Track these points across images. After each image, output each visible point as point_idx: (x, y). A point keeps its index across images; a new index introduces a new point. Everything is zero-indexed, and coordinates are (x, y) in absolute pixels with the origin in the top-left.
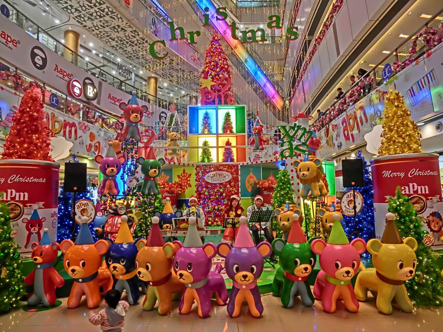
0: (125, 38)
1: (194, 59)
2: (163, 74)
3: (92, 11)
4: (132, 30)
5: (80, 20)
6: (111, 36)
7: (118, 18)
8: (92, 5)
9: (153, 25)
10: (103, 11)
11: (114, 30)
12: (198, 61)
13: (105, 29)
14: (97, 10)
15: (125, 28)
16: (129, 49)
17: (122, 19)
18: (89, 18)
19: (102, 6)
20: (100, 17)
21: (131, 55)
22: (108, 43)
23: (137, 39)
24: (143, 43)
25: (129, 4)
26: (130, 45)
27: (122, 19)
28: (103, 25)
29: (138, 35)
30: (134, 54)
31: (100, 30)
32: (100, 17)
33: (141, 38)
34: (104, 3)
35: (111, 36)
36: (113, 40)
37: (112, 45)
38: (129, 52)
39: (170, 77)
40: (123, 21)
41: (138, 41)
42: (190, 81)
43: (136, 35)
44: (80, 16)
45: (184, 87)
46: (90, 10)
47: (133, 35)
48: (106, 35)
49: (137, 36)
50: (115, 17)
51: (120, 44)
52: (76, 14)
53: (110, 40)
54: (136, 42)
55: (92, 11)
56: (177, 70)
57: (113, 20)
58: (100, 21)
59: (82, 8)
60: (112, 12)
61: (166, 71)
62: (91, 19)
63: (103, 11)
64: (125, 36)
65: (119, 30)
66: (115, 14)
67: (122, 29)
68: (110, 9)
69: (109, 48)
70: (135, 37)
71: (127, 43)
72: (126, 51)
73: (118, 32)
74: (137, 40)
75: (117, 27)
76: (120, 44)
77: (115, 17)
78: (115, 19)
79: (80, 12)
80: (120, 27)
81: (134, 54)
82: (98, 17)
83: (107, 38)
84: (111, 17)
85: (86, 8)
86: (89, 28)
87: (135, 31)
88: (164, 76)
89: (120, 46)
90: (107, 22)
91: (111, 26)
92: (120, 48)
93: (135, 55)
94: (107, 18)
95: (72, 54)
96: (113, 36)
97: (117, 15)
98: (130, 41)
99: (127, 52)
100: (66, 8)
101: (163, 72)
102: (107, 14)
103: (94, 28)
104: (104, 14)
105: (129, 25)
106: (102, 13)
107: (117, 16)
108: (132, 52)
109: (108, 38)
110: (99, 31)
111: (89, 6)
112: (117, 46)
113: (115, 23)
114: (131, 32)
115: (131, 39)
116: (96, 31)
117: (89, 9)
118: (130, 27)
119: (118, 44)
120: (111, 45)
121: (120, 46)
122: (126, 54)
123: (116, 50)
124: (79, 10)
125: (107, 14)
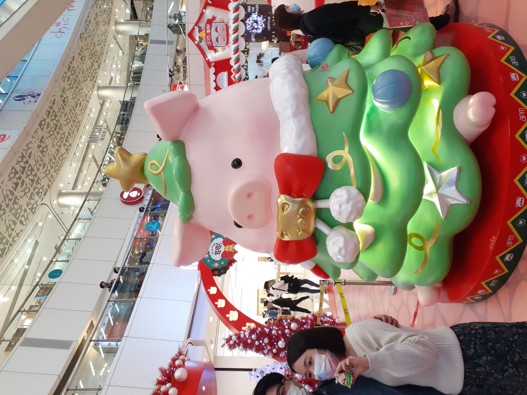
1: (60, 32)
2: (92, 78)
3: (27, 181)
4: (40, 129)
5: (43, 193)
6: (55, 154)
7: (29, 148)
8: (20, 182)
9: (24, 99)
10: (24, 168)
11: (46, 152)
12: (62, 25)
13: (47, 163)
14: (25, 175)
15: (40, 138)
16: (66, 129)
17: (29, 144)
18: (38, 183)
19: (18, 170)
20: (32, 170)
21: (74, 126)
22: (64, 155)
23: (51, 121)
24: (54, 111)
26: (60, 129)
27: (29, 144)
28: (42, 166)
29: (44, 120)
30: (72, 122)
31: (49, 168)
32: (32, 170)
33: (48, 116)
34: (13, 168)
35: (55, 154)
36: (58, 151)
37: (65, 151)
38: (70, 129)
39: (94, 68)
40: (31, 142)
41: (53, 120)
42: (95, 36)
43: (46, 123)
44: (38, 193)
45: (105, 45)
46: (27, 183)
47: (46, 126)
48: (54, 161)
49: (47, 121)
50: (28, 152)
51: (62, 142)
53: (60, 154)
54: (55, 122)
55: (27, 181)
56: (81, 59)
57: (32, 154)
58: (38, 170)
59: (27, 193)
60: (23, 157)
61: (86, 76)
62: (37, 181)
63: (24, 168)
64: (49, 137)
66: (24, 153)
67: (41, 141)
68: (20, 159)
69: (69, 154)
70: (48, 124)
71: (58, 133)
72: (69, 133)
73: (46, 147)
75: (41, 149)
76: (62, 142)
77: (28, 152)
78: (31, 152)
79: (32, 193)
80: (40, 144)
81: (72, 122)
82: (34, 173)
83: (57, 159)
84: (29, 157)
85: (26, 188)
86: (50, 181)
87: (40, 125)
88: (94, 78)
89: (64, 142)
90: (37, 162)
91: (41, 155)
92: (66, 141)
93: (72, 120)
94: (32, 162)
95: (89, 200)
96: (53, 151)
97: (24, 150)
98: (55, 130)
99: (70, 132)
100: (31, 209)
101: (89, 79)
102: (27, 162)
103: (49, 176)
104: (27, 166)
105: (34, 133)
106: (27, 169)
107: (27, 150)
108: (70, 125)
109: (57, 158)
110: (51, 170)
111: (22, 185)
112: (65, 145)
113: (35, 151)
114: (42, 129)
115: (53, 129)
116: (51, 173)
117: (27, 185)
118: (36, 132)
119: (62, 145)
120: (66, 153)
121: (64, 142)
122: (73, 132)
123: (70, 145)
124: (31, 196)
125: (27, 162)
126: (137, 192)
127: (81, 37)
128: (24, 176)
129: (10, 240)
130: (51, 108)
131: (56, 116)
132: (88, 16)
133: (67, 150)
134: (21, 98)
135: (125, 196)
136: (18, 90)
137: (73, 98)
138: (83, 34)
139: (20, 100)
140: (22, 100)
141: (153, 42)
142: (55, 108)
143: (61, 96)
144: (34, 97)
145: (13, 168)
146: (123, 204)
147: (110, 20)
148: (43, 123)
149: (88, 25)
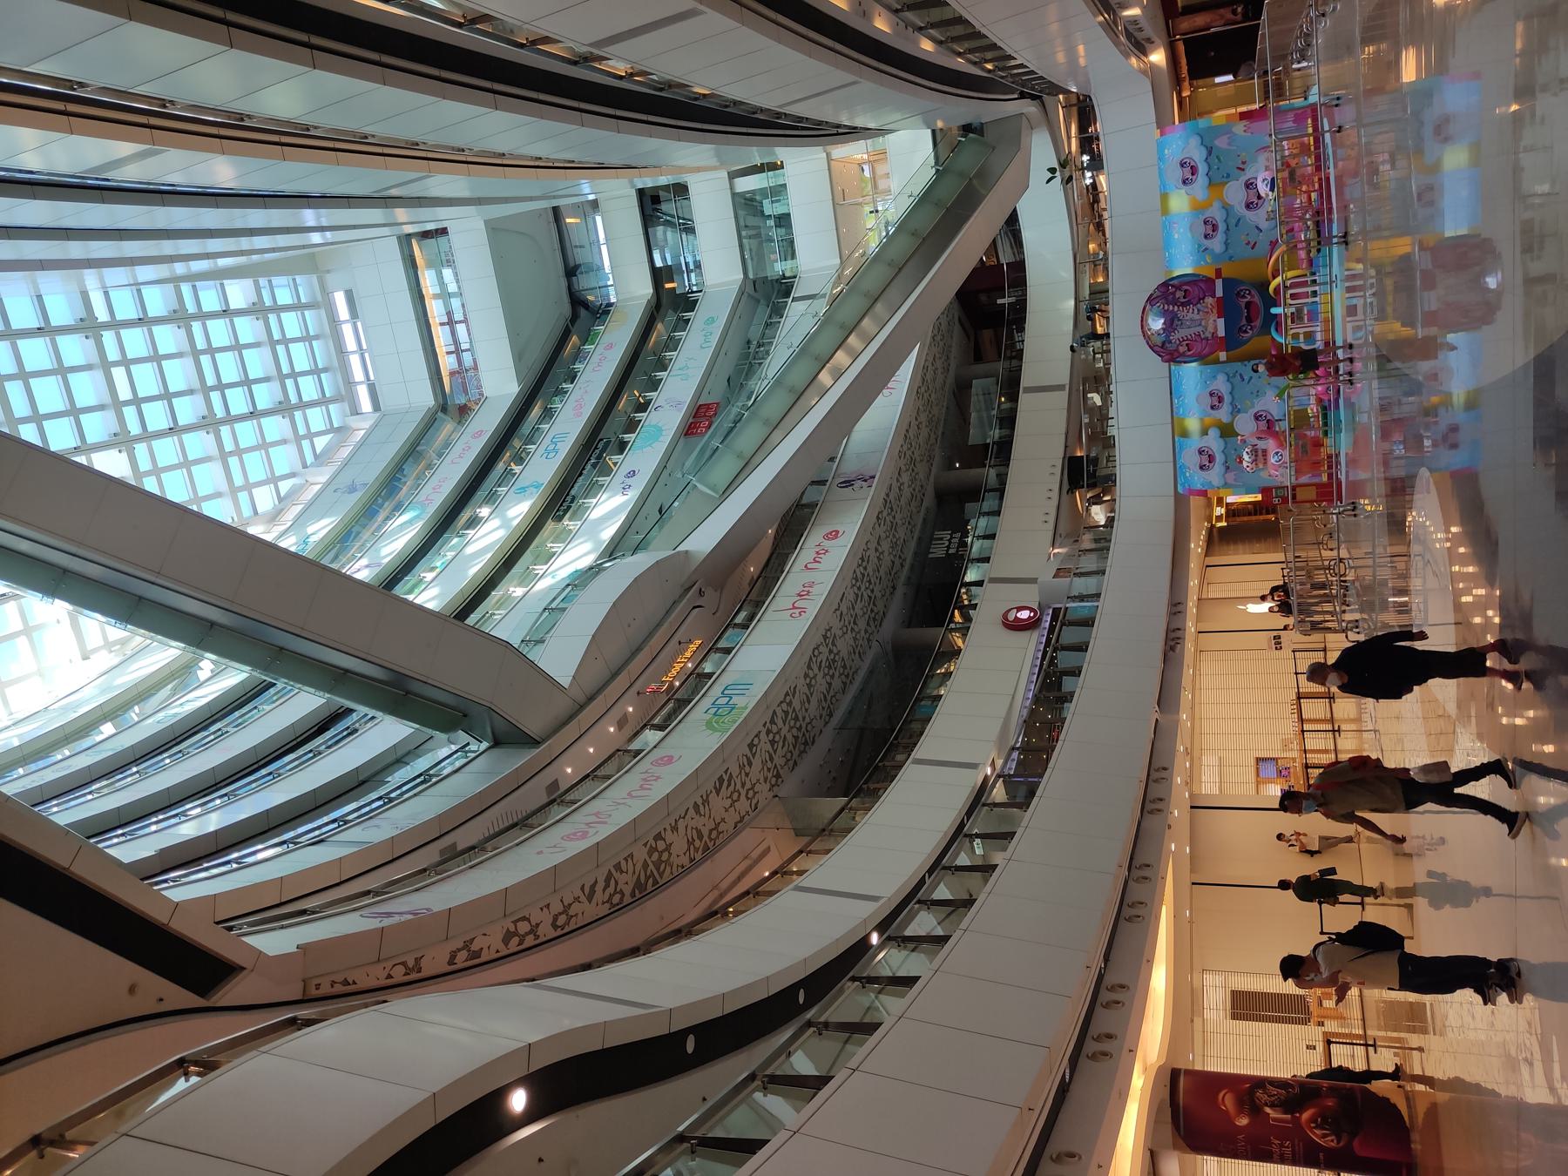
0: (889, 540)
4: (877, 525)
25: (837, 532)
36: (893, 562)
44: (874, 619)
52: (871, 623)
57: (871, 559)
60: (862, 559)
65: (880, 550)
74: (889, 514)
84: (868, 563)
87: (878, 518)
94: (870, 570)
100: (869, 640)
102: (865, 568)
112: (900, 557)
123: (904, 560)
126: (1028, 612)
127: (917, 392)
128: (863, 588)
129: (851, 674)
130: (888, 495)
131: (892, 510)
132: (926, 360)
133: (902, 566)
134: (848, 483)
135: (1011, 617)
136: (842, 474)
137: (909, 486)
138: (920, 387)
139: (846, 487)
140: (850, 486)
141: (1029, 390)
142: (891, 497)
143: (898, 481)
144: (865, 481)
145: (855, 571)
146: (1008, 631)
147: (949, 365)
148: (880, 516)
149: (925, 374)
